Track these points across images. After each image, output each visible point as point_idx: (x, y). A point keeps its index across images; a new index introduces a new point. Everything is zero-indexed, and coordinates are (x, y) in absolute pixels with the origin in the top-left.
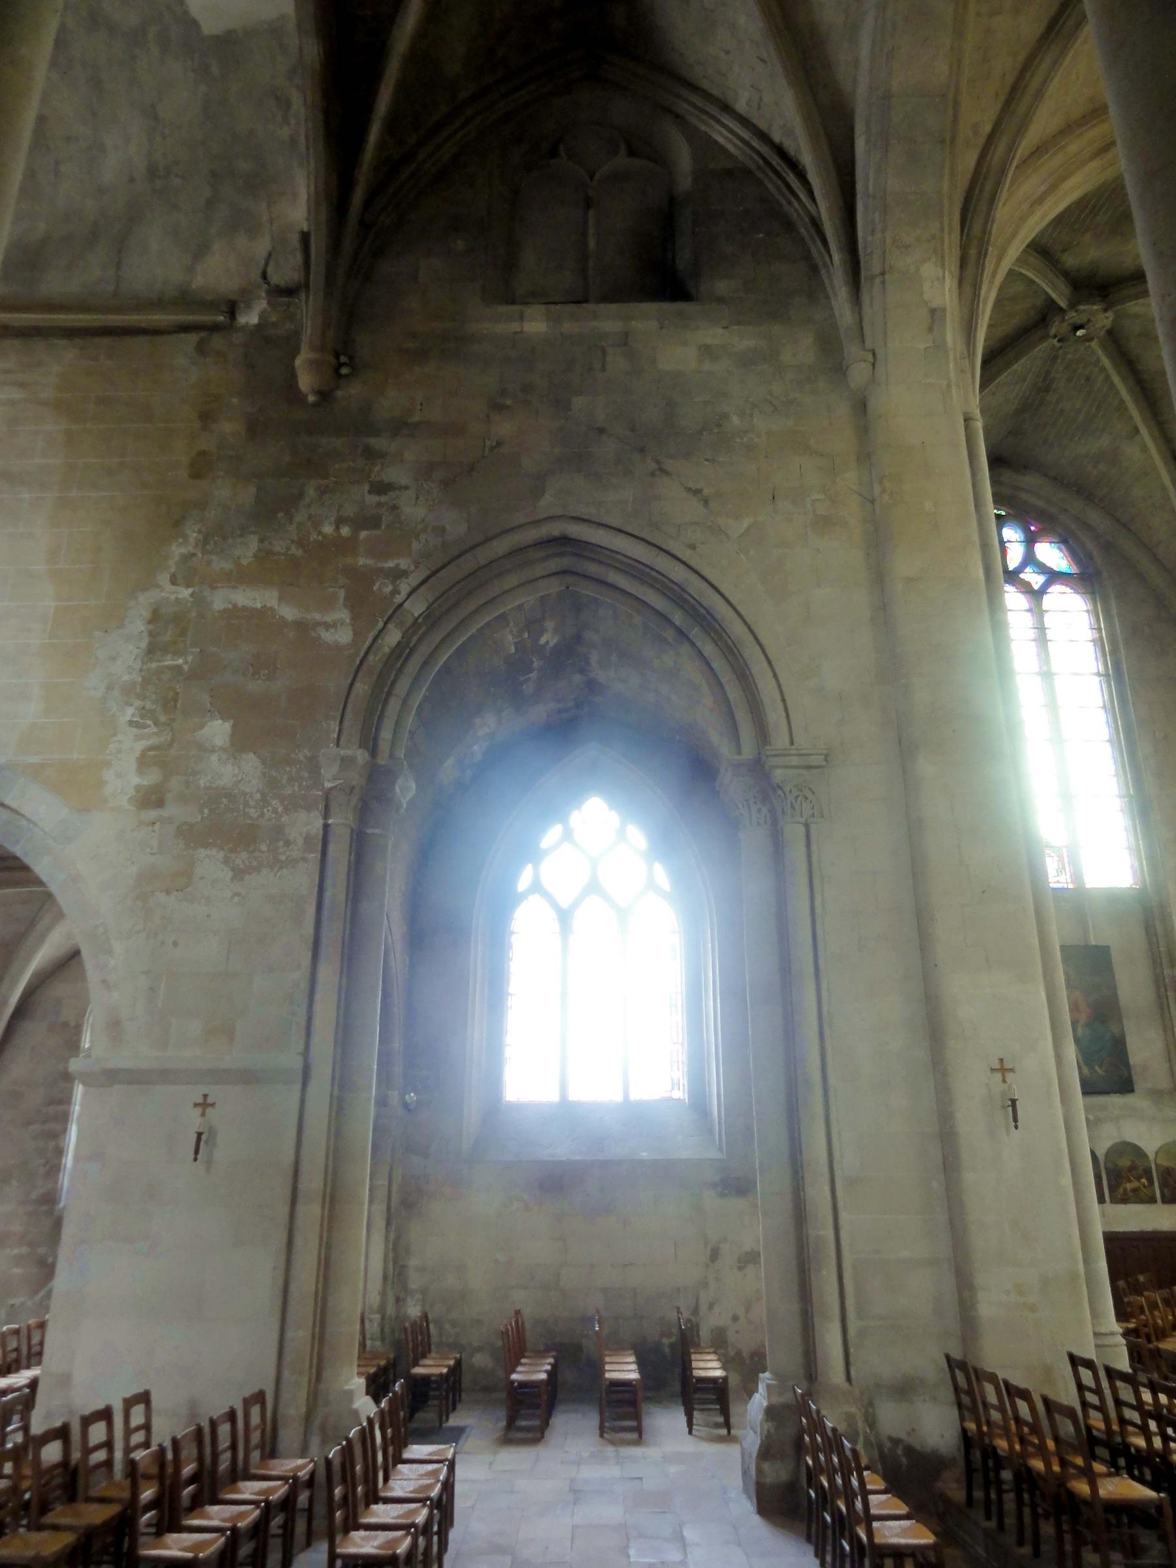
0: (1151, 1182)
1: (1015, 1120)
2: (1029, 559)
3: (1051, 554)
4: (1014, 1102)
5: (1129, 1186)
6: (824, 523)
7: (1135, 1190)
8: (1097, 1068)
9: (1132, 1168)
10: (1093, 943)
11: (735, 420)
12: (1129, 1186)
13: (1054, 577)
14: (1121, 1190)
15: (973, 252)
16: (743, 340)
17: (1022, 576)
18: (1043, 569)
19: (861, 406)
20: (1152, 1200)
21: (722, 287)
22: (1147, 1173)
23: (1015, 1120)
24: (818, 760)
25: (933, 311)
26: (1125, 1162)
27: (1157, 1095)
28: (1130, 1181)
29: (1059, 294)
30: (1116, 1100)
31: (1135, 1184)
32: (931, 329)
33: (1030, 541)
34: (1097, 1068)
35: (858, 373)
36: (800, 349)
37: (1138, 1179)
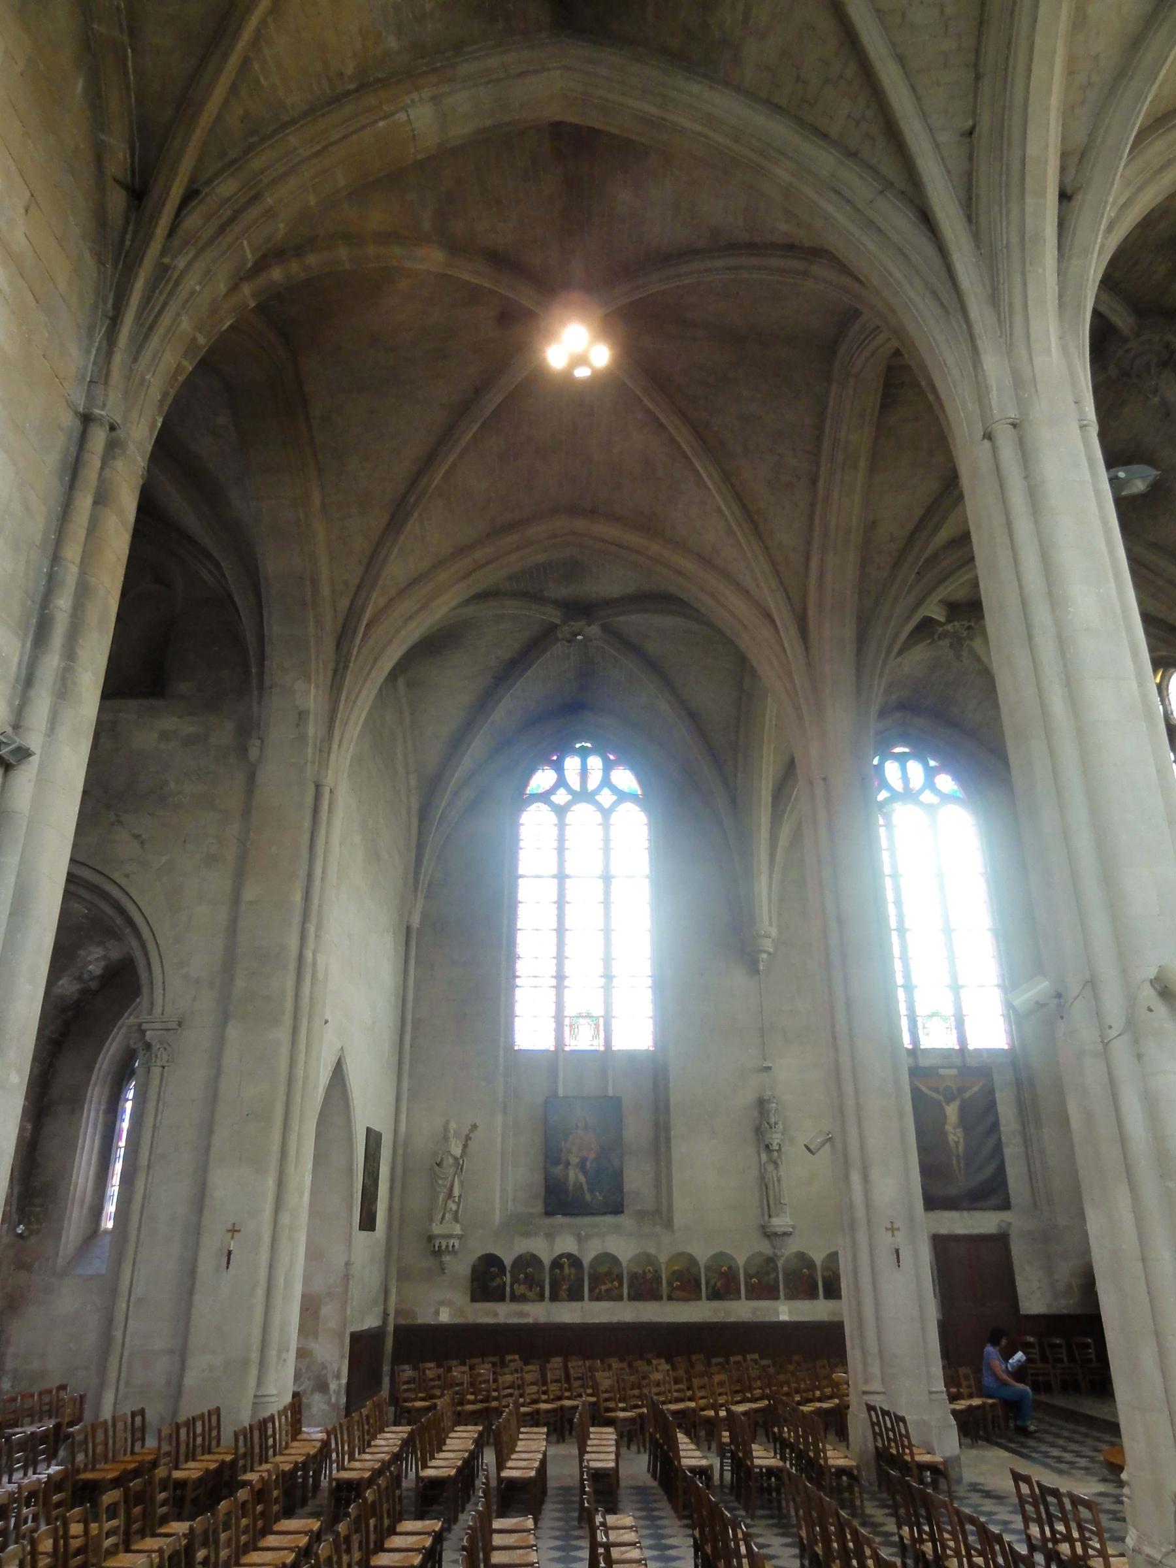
0: (621, 1284)
1: (228, 1263)
2: (606, 782)
3: (625, 778)
4: (230, 1253)
5: (603, 1288)
6: (212, 859)
7: (607, 1291)
9: (608, 1274)
10: (610, 1093)
11: (172, 785)
12: (603, 1288)
13: (623, 796)
15: (341, 665)
16: (188, 727)
17: (597, 797)
18: (614, 789)
19: (251, 778)
20: (620, 1298)
21: (183, 687)
22: (620, 1278)
23: (228, 1263)
24: (175, 1025)
25: (300, 713)
26: (603, 1269)
27: (642, 1215)
28: (605, 1284)
29: (554, 615)
30: (609, 1219)
31: (609, 1286)
32: (298, 725)
33: (608, 767)
35: (254, 753)
36: (224, 733)
37: (612, 1282)
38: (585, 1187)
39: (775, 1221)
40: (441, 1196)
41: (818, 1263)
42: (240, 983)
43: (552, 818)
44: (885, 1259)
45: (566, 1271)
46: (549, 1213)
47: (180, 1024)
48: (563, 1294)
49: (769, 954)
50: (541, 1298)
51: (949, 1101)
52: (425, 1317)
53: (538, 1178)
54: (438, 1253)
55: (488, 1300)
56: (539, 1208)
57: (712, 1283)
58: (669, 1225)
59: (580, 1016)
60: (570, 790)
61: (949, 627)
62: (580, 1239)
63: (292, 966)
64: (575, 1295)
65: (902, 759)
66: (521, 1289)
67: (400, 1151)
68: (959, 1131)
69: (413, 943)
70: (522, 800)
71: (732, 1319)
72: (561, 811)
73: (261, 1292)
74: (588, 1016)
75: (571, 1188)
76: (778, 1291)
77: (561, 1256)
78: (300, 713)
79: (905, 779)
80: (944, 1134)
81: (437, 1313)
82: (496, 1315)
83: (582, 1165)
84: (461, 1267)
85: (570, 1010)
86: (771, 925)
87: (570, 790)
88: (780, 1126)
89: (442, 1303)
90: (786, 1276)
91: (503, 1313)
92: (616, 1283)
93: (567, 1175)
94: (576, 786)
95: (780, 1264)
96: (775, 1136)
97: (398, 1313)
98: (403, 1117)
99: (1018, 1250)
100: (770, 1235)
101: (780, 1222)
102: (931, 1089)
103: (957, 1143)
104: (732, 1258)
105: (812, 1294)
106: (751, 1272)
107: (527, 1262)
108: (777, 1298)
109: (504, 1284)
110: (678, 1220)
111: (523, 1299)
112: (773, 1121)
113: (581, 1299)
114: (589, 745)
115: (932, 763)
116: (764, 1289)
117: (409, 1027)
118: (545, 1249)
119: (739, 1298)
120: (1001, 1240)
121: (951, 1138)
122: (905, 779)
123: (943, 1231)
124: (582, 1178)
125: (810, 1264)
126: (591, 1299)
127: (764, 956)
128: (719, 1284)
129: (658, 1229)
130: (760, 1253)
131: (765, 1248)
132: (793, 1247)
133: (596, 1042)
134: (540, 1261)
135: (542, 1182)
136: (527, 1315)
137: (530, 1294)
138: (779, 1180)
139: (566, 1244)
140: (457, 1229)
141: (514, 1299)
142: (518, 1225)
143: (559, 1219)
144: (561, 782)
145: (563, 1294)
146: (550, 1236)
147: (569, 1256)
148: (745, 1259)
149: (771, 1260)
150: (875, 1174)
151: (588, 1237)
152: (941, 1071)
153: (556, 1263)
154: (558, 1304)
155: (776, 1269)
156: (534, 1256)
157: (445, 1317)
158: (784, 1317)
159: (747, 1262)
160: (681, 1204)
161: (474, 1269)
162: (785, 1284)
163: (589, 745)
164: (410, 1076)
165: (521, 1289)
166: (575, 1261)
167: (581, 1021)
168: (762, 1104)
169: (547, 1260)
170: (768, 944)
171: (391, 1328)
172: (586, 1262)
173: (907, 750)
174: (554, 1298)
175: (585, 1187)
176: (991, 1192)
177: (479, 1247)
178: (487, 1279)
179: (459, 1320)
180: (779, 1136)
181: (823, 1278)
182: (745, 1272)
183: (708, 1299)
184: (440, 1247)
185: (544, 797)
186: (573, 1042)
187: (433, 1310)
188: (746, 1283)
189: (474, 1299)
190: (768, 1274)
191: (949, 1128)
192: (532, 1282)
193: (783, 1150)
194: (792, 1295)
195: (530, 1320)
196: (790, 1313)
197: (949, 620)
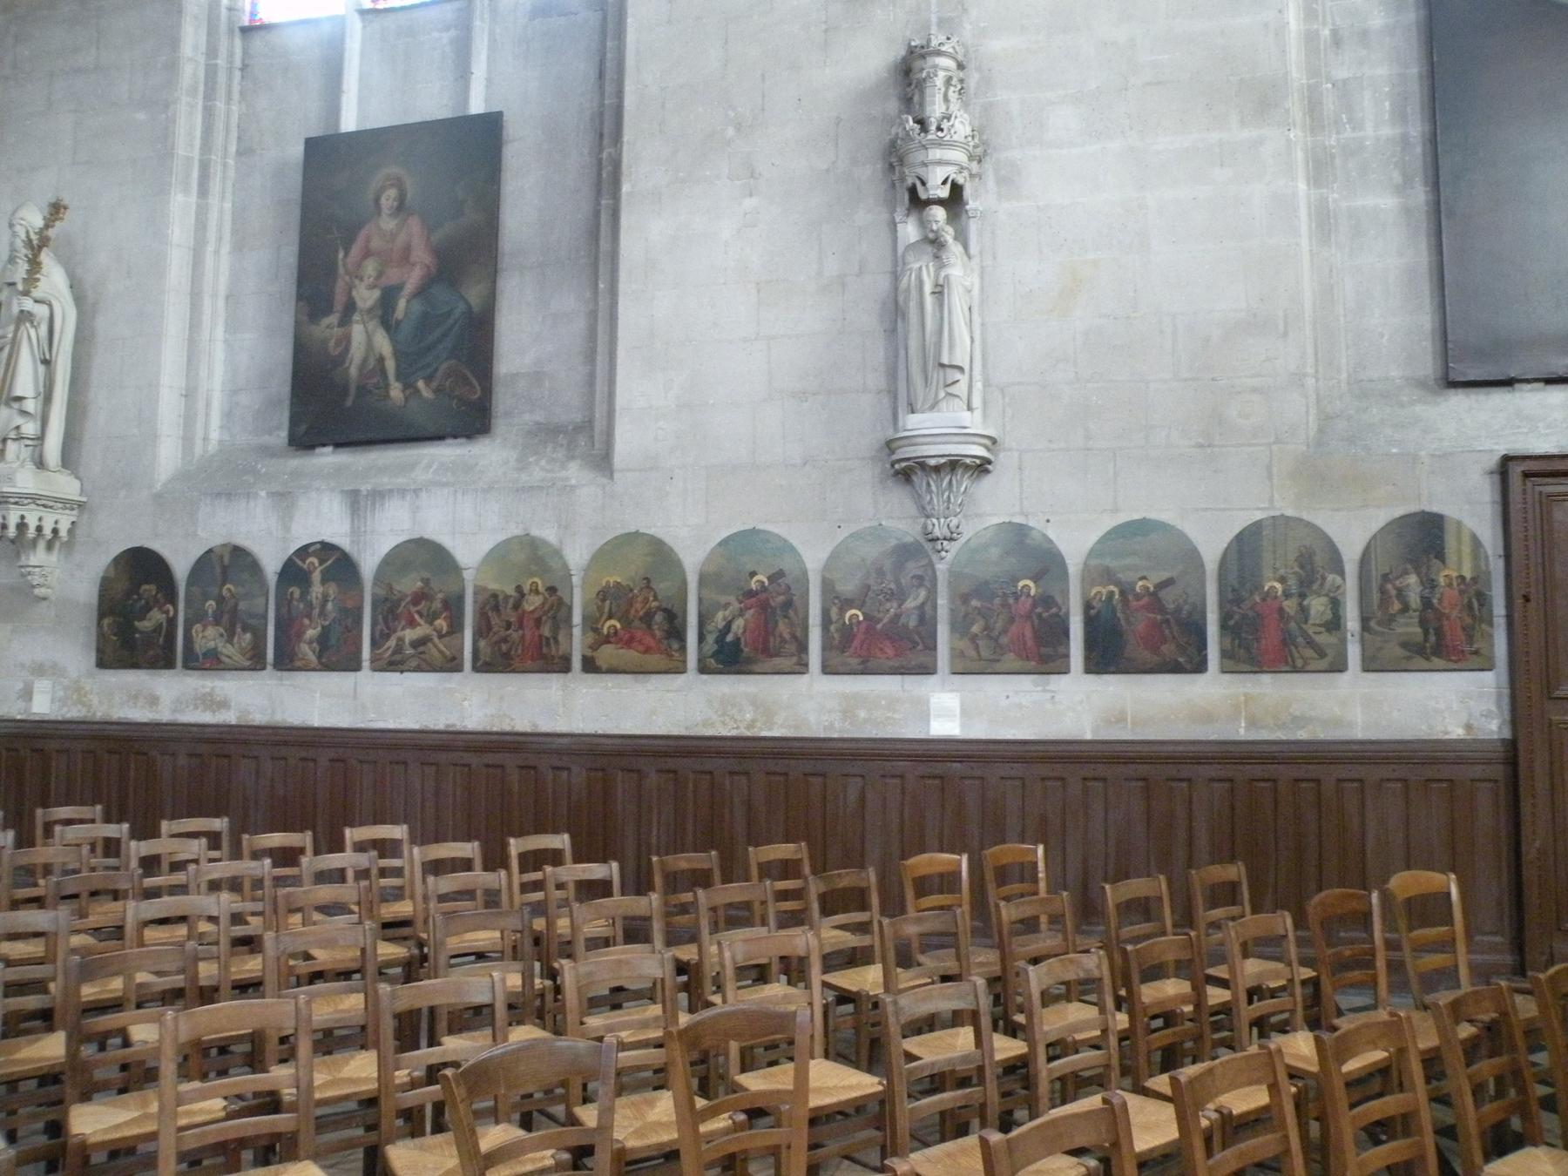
0: (456, 627)
5: (410, 635)
7: (419, 643)
8: (421, 384)
9: (419, 597)
12: (410, 635)
14: (392, 643)
20: (452, 665)
22: (453, 606)
26: (409, 584)
28: (412, 623)
34: (421, 384)
38: (390, 365)
39: (915, 423)
41: (1074, 566)
45: (317, 590)
46: (304, 438)
48: (307, 651)
50: (256, 662)
55: (135, 666)
57: (719, 619)
58: (603, 461)
62: (358, 503)
64: (337, 655)
66: (208, 637)
71: (778, 730)
75: (353, 371)
77: (303, 551)
81: (27, 694)
82: (154, 701)
83: (384, 311)
84: (73, 580)
88: (961, 127)
89: (40, 670)
91: (165, 698)
92: (441, 623)
93: (347, 339)
96: (936, 154)
100: (908, 472)
101: (939, 426)
104: (787, 548)
105: (1044, 654)
106: (848, 587)
108: (928, 670)
109: (172, 622)
110: (627, 441)
111: (209, 662)
112: (935, 110)
113: (353, 665)
116: (883, 639)
118: (269, 538)
119: (801, 668)
123: (1543, 444)
125: (1048, 563)
128: (738, 626)
129: (575, 472)
130: (877, 532)
131: (896, 515)
132: (987, 509)
134: (254, 567)
136: (223, 705)
137: (228, 651)
138: (939, 292)
139: (322, 519)
140: (68, 486)
142: (223, 478)
143: (327, 458)
145: (307, 651)
146: (284, 499)
147: (327, 548)
148: (824, 555)
151: (378, 496)
153: (293, 572)
154: (301, 678)
155: (927, 580)
156: (238, 552)
157: (43, 705)
159: (834, 556)
160: (638, 391)
161: (105, 585)
162: (960, 626)
165: (208, 637)
166: (338, 563)
168: (908, 76)
169: (272, 565)
172: (368, 565)
174: (287, 661)
175: (390, 365)
177: (116, 535)
178: (139, 610)
179: (73, 712)
180: (959, 156)
181: (1088, 606)
182: (827, 586)
183: (703, 669)
184: (22, 526)
187: (20, 685)
188: (826, 622)
189: (102, 664)
190: (899, 595)
192: (231, 619)
193: (972, 204)
194: (978, 661)
195: (229, 717)
196: (966, 712)
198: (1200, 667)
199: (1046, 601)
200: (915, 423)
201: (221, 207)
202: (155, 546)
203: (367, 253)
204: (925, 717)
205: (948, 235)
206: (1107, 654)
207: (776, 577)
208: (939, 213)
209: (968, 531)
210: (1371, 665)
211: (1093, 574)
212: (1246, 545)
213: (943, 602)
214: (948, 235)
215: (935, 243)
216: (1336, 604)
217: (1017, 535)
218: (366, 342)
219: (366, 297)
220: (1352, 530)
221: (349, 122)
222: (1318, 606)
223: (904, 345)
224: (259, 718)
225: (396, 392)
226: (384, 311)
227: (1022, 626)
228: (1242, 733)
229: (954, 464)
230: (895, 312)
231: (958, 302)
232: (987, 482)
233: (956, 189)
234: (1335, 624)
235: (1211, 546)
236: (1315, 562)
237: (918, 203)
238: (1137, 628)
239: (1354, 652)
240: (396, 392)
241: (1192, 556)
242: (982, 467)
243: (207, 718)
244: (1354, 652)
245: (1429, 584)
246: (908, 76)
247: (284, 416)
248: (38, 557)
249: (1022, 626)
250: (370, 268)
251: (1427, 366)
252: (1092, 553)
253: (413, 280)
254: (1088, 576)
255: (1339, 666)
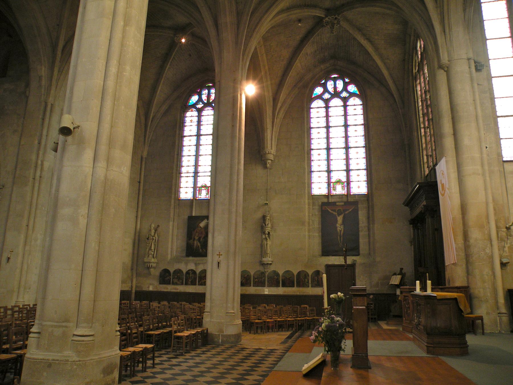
25: (40, 77)
39: (264, 259)
40: (147, 249)
41: (281, 275)
42: (18, 172)
43: (195, 113)
44: (215, 266)
45: (191, 275)
46: (188, 255)
47: (3, 186)
49: (272, 160)
50: (182, 284)
51: (339, 215)
52: (145, 289)
53: (185, 244)
54: (148, 268)
55: (165, 284)
56: (184, 254)
59: (202, 187)
60: (203, 103)
61: (327, 19)
62: (196, 265)
63: (33, 166)
64: (193, 283)
65: (335, 80)
67: (137, 234)
68: (342, 227)
69: (144, 163)
70: (186, 108)
72: (200, 111)
73: (18, 270)
74: (205, 186)
76: (265, 284)
77: (189, 270)
78: (40, 77)
79: (335, 88)
80: (336, 228)
81: (149, 287)
82: (168, 289)
83: (199, 240)
84: (156, 272)
85: (199, 185)
86: (271, 149)
87: (203, 103)
88: (270, 225)
89: (151, 284)
90: (268, 278)
91: (169, 288)
93: (194, 243)
94: (206, 102)
95: (267, 274)
97: (136, 287)
98: (139, 223)
99: (358, 270)
100: (263, 264)
101: (267, 260)
102: (332, 210)
103: (341, 231)
105: (277, 285)
107: (178, 272)
111: (176, 284)
112: (267, 223)
113: (195, 284)
114: (211, 85)
115: (347, 80)
117: (141, 192)
119: (250, 286)
120: (353, 266)
121: (339, 229)
122: (335, 88)
123: (330, 263)
124: (199, 244)
125: (278, 275)
126: (199, 285)
127: (270, 161)
130: (259, 271)
131: (261, 269)
132: (272, 268)
133: (207, 196)
134: (182, 272)
135: (186, 246)
136: (178, 289)
137: (178, 282)
138: (267, 245)
139: (191, 266)
141: (173, 284)
142: (177, 260)
143: (191, 258)
144: (200, 100)
145: (189, 283)
146: (186, 264)
147: (192, 270)
149: (263, 273)
150: (216, 234)
151: (199, 264)
152: (337, 204)
153: (188, 273)
155: (264, 276)
156: (180, 270)
157: (151, 289)
158: (266, 293)
159: (254, 274)
162: (268, 281)
163: (211, 85)
164: (142, 209)
165: (176, 281)
166: (194, 272)
167: (203, 189)
168: (264, 217)
169: (184, 272)
170: (271, 157)
171: (134, 291)
172: (198, 272)
173: (336, 76)
174: (186, 284)
176: (353, 249)
177: (163, 267)
178: (165, 277)
179: (155, 290)
180: (270, 229)
182: (254, 277)
185: (194, 106)
186: (199, 196)
189: (160, 284)
191: (338, 225)
192: (179, 278)
194: (270, 285)
195: (179, 291)
196: (269, 291)
197: (326, 16)
198: (294, 286)
199: (277, 279)
200: (264, 259)
201: (176, 224)
202: (165, 268)
203: (197, 232)
204: (264, 292)
205: (268, 238)
206: (284, 285)
207: (248, 275)
208: (267, 235)
209: (269, 271)
210: (312, 287)
211: (283, 276)
212: (299, 273)
213: (266, 279)
214: (268, 238)
215: (267, 239)
216: (308, 280)
217: (274, 272)
218: (196, 244)
219: (197, 238)
220: (310, 272)
221: (194, 215)
222: (306, 280)
223: (262, 251)
224: (182, 291)
225: (201, 250)
226: (199, 240)
227: (275, 280)
228: (298, 294)
229: (268, 264)
230: (262, 246)
231: (268, 246)
232: (271, 266)
233: (269, 233)
234: (308, 282)
235: (295, 273)
236: (306, 275)
237: (264, 233)
238: (288, 282)
239: (310, 285)
240: (201, 250)
241: (293, 275)
242: (271, 264)
243: (175, 291)
244: (310, 285)
245: (318, 278)
246: (264, 217)
247: (185, 252)
248: (152, 270)
249: (275, 280)
250: (197, 234)
251: (320, 253)
252: (283, 273)
253: (203, 236)
254: (282, 276)
255: (309, 287)
